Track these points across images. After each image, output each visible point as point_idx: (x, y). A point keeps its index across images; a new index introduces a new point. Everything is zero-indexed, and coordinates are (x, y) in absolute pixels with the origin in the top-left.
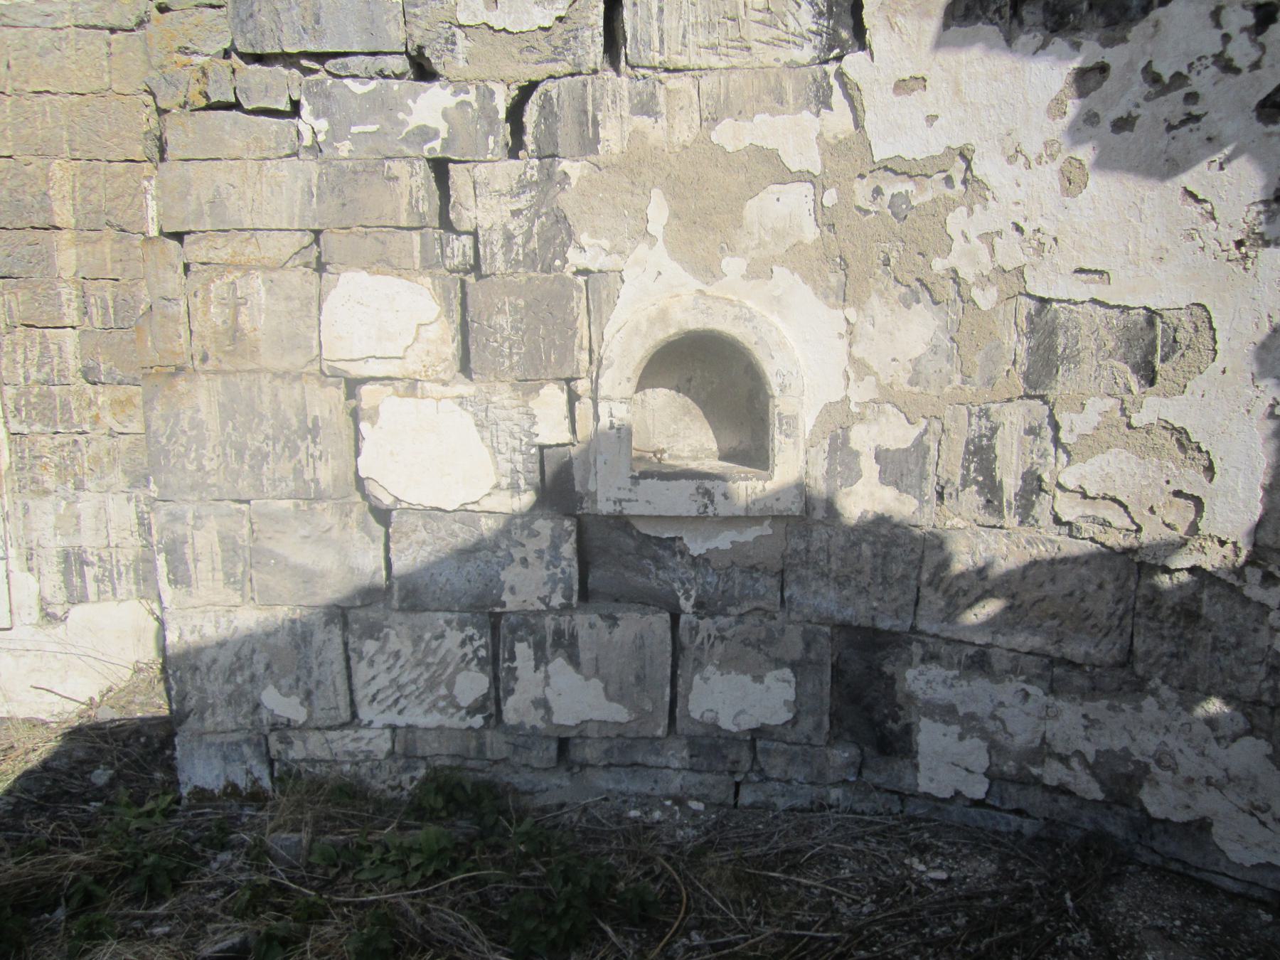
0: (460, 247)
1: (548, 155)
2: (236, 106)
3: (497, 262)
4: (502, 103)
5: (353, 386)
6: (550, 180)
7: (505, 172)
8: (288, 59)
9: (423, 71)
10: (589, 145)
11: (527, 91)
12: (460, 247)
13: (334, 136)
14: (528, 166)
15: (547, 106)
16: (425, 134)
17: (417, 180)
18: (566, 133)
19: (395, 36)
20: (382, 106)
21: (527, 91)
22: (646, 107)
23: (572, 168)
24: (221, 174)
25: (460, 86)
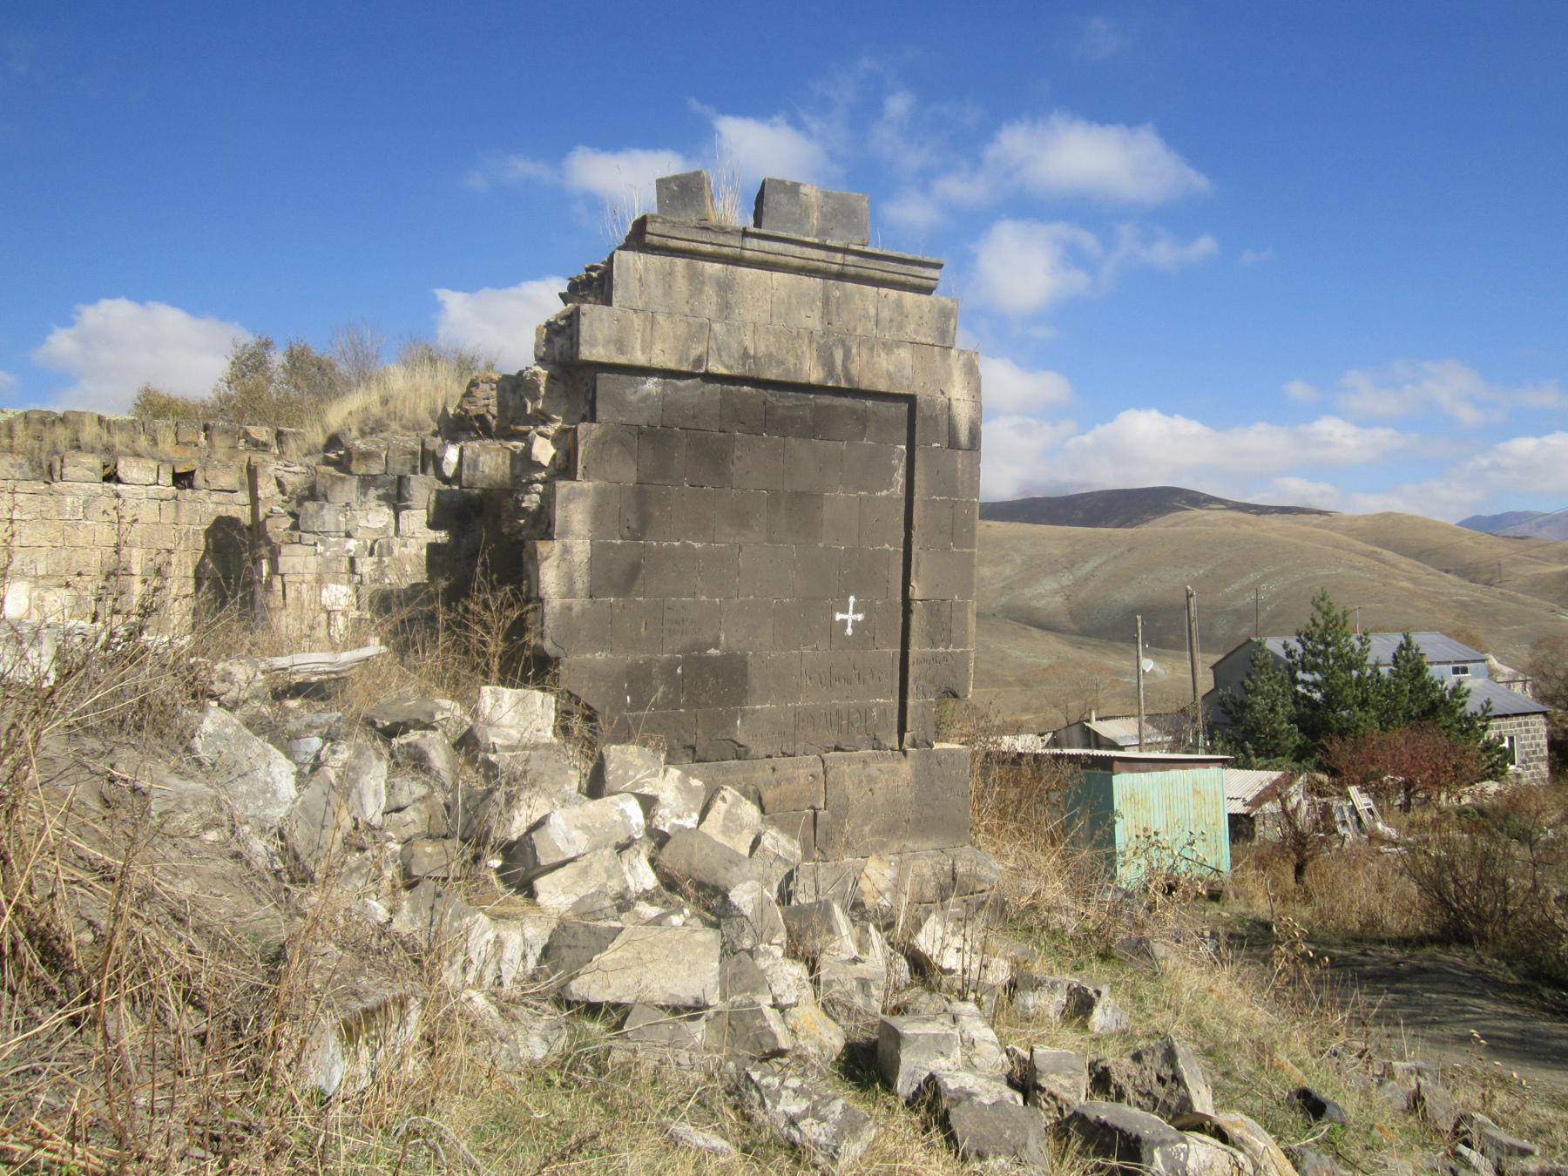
0: (357, 578)
1: (381, 555)
2: (300, 543)
3: (367, 580)
4: (369, 543)
5: (329, 613)
6: (380, 562)
7: (370, 560)
8: (315, 533)
9: (348, 535)
10: (390, 552)
11: (375, 541)
12: (357, 578)
13: (326, 551)
14: (375, 559)
15: (380, 546)
16: (349, 551)
17: (345, 563)
18: (385, 551)
19: (343, 528)
20: (338, 544)
21: (375, 541)
22: (405, 545)
23: (386, 560)
24: (296, 560)
25: (359, 540)
